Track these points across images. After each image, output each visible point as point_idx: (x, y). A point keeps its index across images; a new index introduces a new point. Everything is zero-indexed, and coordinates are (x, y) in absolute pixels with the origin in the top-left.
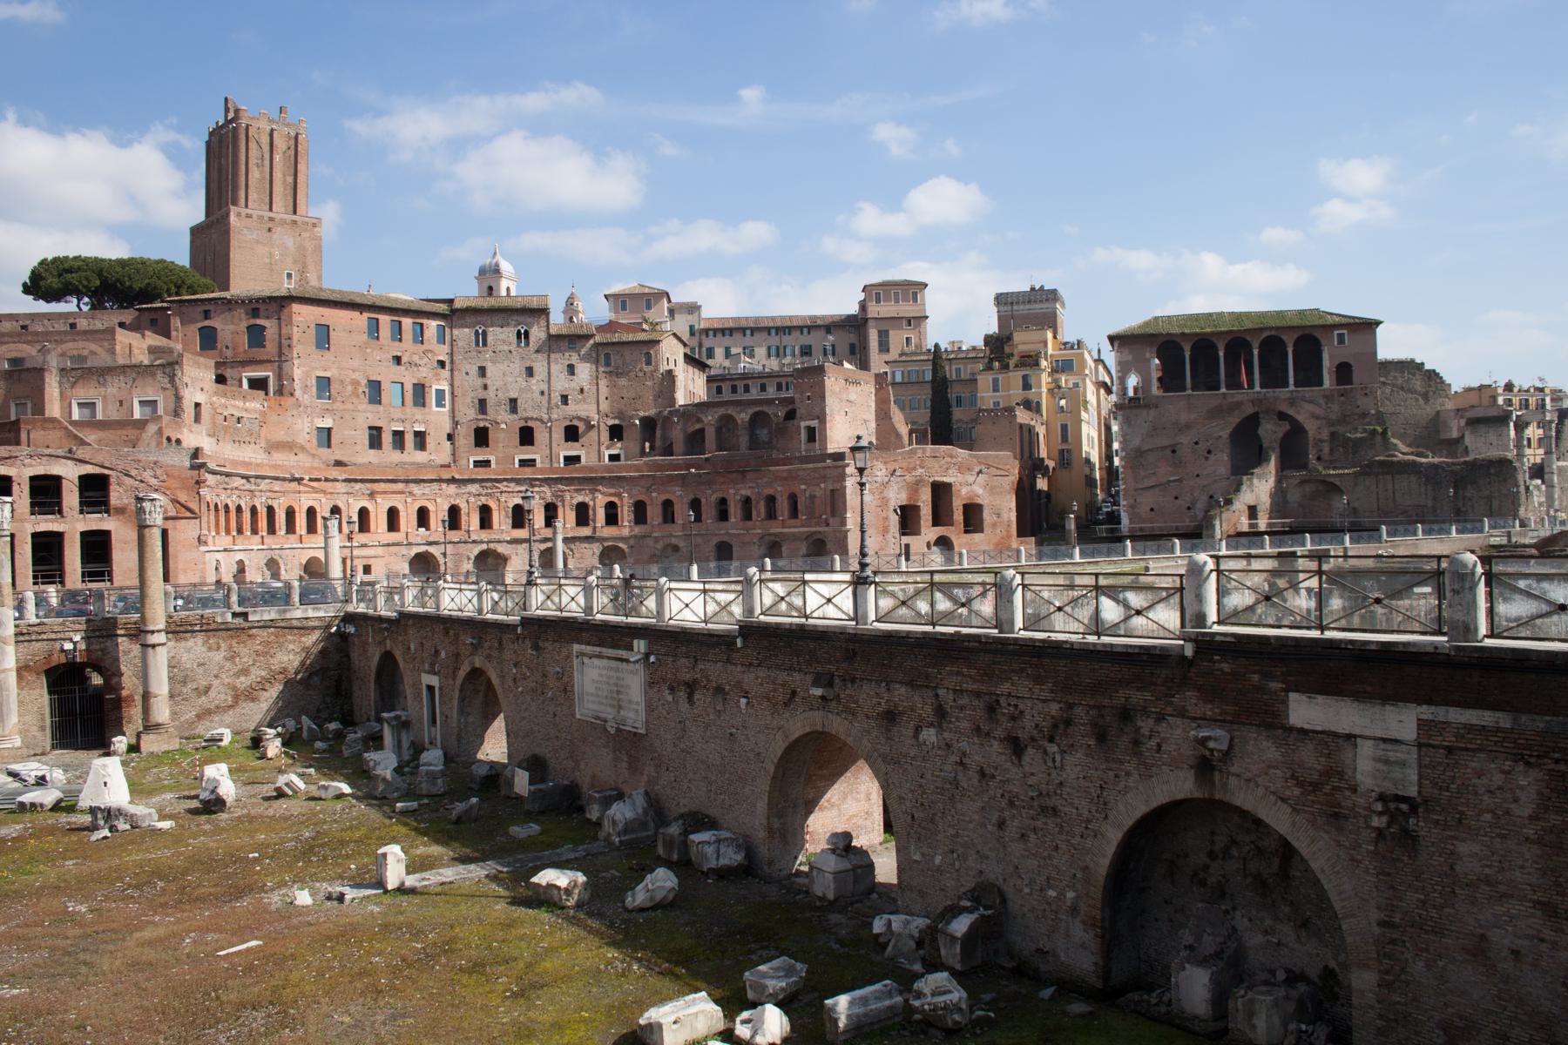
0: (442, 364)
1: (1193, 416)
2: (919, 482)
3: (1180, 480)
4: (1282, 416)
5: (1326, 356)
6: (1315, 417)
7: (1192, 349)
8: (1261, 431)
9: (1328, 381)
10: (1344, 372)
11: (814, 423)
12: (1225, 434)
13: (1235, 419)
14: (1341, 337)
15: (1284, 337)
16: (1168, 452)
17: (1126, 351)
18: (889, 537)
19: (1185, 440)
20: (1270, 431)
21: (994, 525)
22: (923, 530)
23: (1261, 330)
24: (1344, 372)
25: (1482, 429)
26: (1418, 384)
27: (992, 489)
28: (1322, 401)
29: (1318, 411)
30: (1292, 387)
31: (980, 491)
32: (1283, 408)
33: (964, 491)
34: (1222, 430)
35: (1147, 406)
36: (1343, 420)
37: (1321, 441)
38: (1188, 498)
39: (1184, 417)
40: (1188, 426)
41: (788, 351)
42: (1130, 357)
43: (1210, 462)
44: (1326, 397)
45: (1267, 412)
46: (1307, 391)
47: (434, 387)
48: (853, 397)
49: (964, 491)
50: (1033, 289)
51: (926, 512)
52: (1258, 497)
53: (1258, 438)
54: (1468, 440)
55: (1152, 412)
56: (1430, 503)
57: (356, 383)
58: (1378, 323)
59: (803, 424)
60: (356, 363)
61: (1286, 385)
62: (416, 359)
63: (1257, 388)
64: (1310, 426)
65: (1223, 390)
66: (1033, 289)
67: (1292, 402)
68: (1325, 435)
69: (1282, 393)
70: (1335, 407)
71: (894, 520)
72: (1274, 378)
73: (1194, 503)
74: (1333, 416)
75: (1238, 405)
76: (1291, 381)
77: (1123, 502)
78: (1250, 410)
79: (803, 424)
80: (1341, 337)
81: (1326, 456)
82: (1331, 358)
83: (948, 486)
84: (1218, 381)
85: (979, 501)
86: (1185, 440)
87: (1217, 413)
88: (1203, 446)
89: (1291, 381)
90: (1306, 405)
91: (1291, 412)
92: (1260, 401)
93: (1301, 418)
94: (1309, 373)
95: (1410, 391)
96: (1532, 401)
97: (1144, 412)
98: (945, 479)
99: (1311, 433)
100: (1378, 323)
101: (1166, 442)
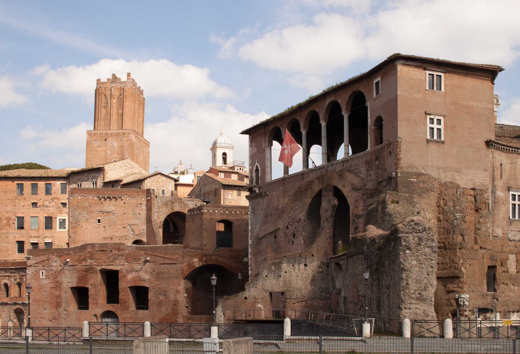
0: (64, 204)
2: (89, 270)
6: (355, 189)
16: (272, 238)
19: (281, 225)
21: (160, 304)
27: (158, 275)
29: (356, 181)
31: (147, 277)
33: (130, 277)
37: (358, 216)
40: (283, 211)
43: (294, 246)
47: (58, 218)
55: (265, 200)
57: (9, 219)
60: (9, 208)
62: (47, 203)
74: (370, 186)
78: (317, 190)
83: (115, 273)
85: (146, 285)
88: (291, 229)
91: (340, 187)
92: (322, 176)
93: (346, 191)
98: (112, 268)
99: (351, 208)
101: (271, 229)
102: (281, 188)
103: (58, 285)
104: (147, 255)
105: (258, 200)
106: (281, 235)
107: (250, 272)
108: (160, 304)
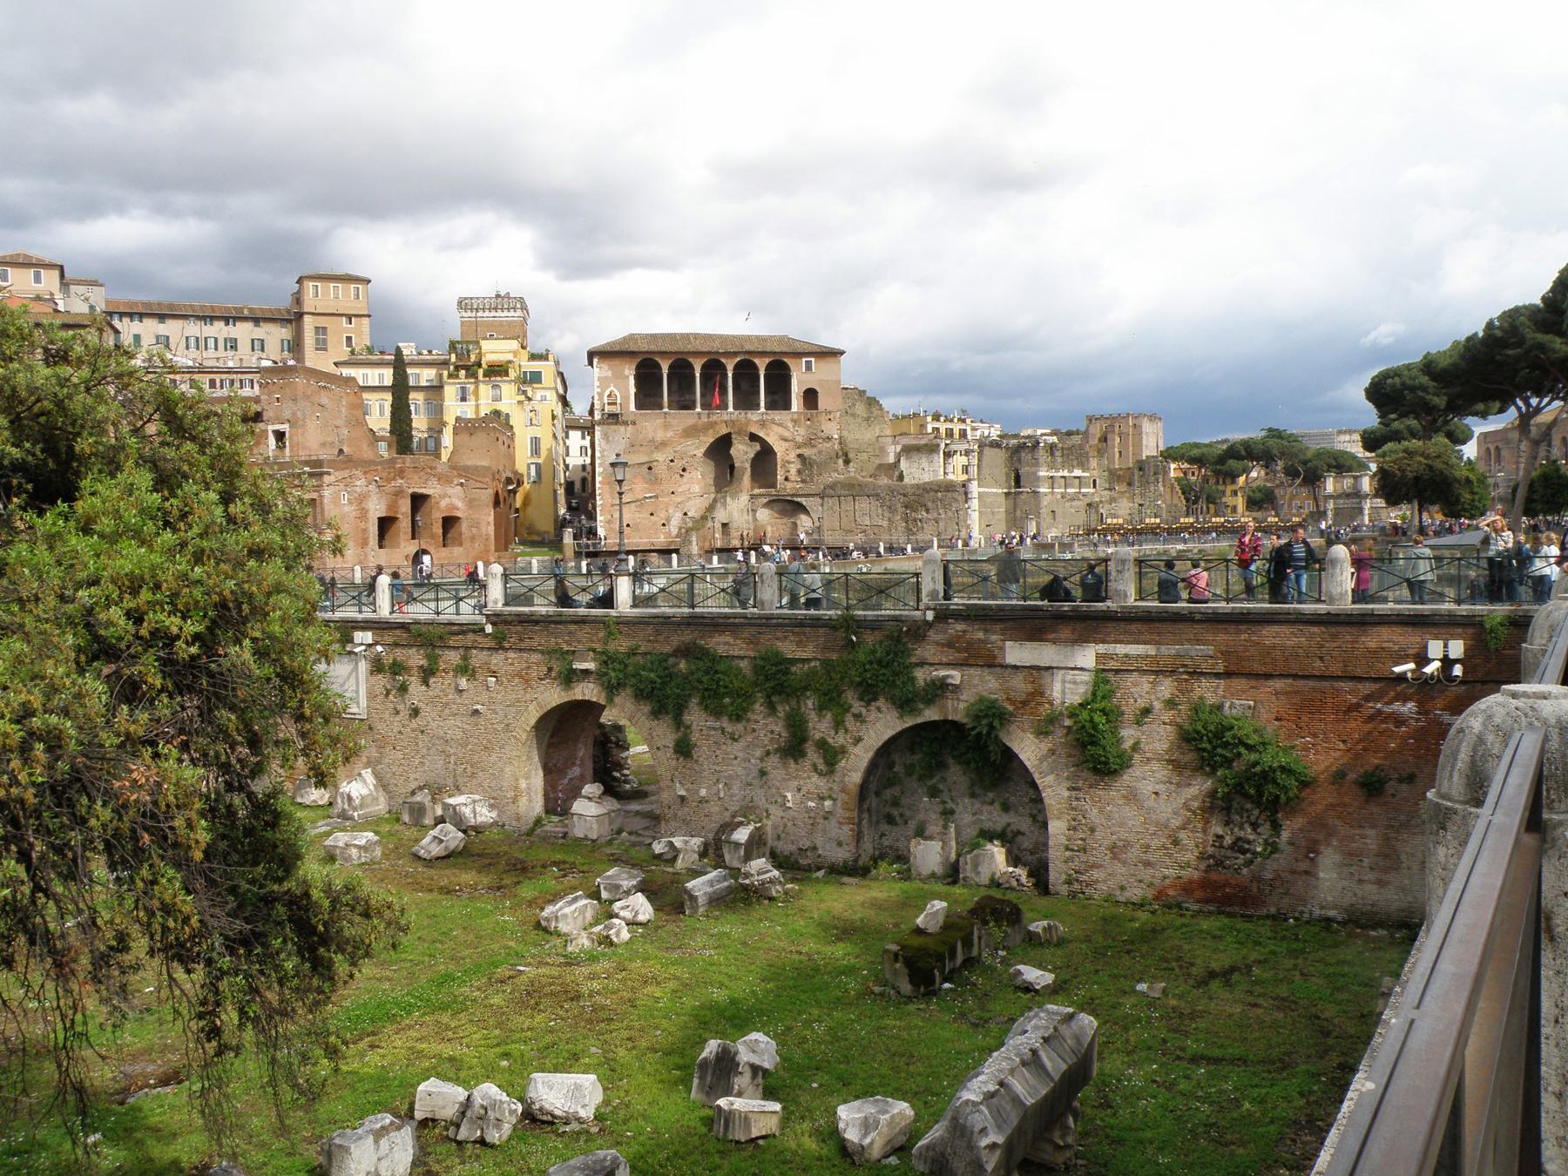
1: (670, 434)
2: (399, 493)
3: (656, 497)
4: (754, 437)
5: (794, 382)
6: (786, 440)
7: (671, 367)
8: (732, 451)
9: (796, 403)
10: (811, 397)
11: (284, 427)
12: (700, 452)
13: (710, 439)
14: (808, 364)
15: (757, 361)
17: (605, 366)
18: (368, 550)
20: (742, 452)
22: (403, 544)
23: (735, 354)
24: (811, 397)
25: (915, 456)
26: (860, 409)
27: (471, 503)
28: (790, 425)
29: (787, 434)
30: (763, 409)
31: (460, 504)
32: (754, 430)
33: (443, 504)
34: (698, 447)
35: (625, 423)
36: (809, 443)
38: (663, 515)
39: (660, 436)
40: (664, 444)
41: (211, 343)
42: (609, 373)
44: (795, 421)
45: (739, 433)
46: (778, 415)
48: (325, 401)
49: (443, 504)
50: (498, 296)
51: (404, 524)
52: (731, 515)
53: (730, 458)
54: (904, 465)
55: (630, 428)
56: (885, 524)
58: (842, 353)
59: (271, 428)
61: (757, 407)
63: (731, 409)
64: (779, 448)
65: (698, 410)
66: (498, 296)
67: (763, 424)
68: (792, 456)
69: (754, 416)
70: (802, 431)
71: (373, 529)
72: (746, 400)
73: (668, 520)
74: (799, 439)
75: (712, 425)
76: (762, 404)
77: (599, 518)
78: (724, 431)
79: (271, 428)
80: (808, 364)
81: (792, 478)
82: (799, 383)
84: (694, 402)
85: (459, 514)
86: (661, 457)
87: (691, 432)
88: (679, 464)
89: (762, 404)
90: (775, 428)
91: (761, 435)
93: (770, 440)
94: (779, 399)
95: (853, 415)
96: (956, 432)
97: (622, 428)
100: (842, 353)
102: (660, 421)
103: (363, 515)
104: (460, 476)
105: (614, 427)
106: (660, 469)
107: (599, 503)
108: (473, 539)
